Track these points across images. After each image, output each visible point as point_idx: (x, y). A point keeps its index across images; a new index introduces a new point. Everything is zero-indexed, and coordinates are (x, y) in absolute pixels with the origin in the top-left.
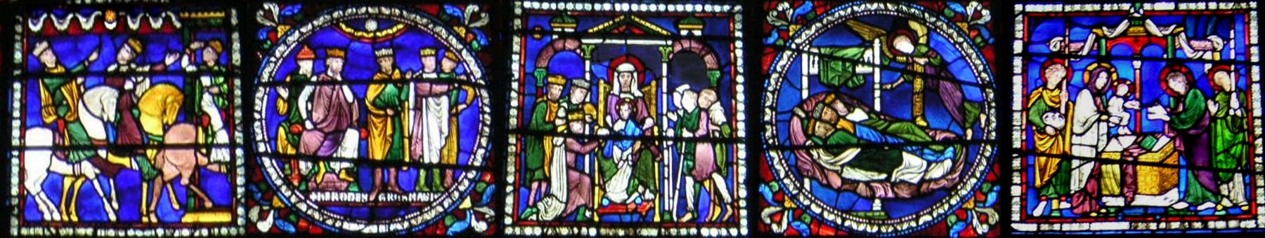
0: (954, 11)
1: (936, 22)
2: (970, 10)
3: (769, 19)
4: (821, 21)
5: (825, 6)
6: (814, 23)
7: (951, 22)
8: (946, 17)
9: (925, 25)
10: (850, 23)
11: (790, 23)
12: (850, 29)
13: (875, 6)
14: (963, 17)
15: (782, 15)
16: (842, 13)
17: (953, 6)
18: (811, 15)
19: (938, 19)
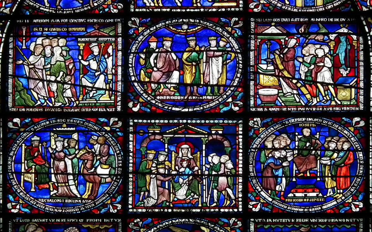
0: (223, 221)
1: (214, 227)
2: (231, 222)
3: (130, 226)
4: (156, 227)
5: (158, 220)
6: (153, 228)
7: (221, 227)
8: (219, 225)
9: (208, 228)
10: (171, 228)
11: (141, 228)
12: (171, 230)
13: (184, 220)
14: (228, 225)
15: (137, 224)
16: (167, 223)
17: (223, 220)
18: (151, 224)
19: (215, 226)
